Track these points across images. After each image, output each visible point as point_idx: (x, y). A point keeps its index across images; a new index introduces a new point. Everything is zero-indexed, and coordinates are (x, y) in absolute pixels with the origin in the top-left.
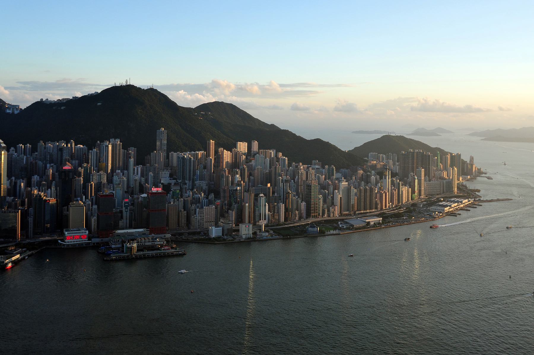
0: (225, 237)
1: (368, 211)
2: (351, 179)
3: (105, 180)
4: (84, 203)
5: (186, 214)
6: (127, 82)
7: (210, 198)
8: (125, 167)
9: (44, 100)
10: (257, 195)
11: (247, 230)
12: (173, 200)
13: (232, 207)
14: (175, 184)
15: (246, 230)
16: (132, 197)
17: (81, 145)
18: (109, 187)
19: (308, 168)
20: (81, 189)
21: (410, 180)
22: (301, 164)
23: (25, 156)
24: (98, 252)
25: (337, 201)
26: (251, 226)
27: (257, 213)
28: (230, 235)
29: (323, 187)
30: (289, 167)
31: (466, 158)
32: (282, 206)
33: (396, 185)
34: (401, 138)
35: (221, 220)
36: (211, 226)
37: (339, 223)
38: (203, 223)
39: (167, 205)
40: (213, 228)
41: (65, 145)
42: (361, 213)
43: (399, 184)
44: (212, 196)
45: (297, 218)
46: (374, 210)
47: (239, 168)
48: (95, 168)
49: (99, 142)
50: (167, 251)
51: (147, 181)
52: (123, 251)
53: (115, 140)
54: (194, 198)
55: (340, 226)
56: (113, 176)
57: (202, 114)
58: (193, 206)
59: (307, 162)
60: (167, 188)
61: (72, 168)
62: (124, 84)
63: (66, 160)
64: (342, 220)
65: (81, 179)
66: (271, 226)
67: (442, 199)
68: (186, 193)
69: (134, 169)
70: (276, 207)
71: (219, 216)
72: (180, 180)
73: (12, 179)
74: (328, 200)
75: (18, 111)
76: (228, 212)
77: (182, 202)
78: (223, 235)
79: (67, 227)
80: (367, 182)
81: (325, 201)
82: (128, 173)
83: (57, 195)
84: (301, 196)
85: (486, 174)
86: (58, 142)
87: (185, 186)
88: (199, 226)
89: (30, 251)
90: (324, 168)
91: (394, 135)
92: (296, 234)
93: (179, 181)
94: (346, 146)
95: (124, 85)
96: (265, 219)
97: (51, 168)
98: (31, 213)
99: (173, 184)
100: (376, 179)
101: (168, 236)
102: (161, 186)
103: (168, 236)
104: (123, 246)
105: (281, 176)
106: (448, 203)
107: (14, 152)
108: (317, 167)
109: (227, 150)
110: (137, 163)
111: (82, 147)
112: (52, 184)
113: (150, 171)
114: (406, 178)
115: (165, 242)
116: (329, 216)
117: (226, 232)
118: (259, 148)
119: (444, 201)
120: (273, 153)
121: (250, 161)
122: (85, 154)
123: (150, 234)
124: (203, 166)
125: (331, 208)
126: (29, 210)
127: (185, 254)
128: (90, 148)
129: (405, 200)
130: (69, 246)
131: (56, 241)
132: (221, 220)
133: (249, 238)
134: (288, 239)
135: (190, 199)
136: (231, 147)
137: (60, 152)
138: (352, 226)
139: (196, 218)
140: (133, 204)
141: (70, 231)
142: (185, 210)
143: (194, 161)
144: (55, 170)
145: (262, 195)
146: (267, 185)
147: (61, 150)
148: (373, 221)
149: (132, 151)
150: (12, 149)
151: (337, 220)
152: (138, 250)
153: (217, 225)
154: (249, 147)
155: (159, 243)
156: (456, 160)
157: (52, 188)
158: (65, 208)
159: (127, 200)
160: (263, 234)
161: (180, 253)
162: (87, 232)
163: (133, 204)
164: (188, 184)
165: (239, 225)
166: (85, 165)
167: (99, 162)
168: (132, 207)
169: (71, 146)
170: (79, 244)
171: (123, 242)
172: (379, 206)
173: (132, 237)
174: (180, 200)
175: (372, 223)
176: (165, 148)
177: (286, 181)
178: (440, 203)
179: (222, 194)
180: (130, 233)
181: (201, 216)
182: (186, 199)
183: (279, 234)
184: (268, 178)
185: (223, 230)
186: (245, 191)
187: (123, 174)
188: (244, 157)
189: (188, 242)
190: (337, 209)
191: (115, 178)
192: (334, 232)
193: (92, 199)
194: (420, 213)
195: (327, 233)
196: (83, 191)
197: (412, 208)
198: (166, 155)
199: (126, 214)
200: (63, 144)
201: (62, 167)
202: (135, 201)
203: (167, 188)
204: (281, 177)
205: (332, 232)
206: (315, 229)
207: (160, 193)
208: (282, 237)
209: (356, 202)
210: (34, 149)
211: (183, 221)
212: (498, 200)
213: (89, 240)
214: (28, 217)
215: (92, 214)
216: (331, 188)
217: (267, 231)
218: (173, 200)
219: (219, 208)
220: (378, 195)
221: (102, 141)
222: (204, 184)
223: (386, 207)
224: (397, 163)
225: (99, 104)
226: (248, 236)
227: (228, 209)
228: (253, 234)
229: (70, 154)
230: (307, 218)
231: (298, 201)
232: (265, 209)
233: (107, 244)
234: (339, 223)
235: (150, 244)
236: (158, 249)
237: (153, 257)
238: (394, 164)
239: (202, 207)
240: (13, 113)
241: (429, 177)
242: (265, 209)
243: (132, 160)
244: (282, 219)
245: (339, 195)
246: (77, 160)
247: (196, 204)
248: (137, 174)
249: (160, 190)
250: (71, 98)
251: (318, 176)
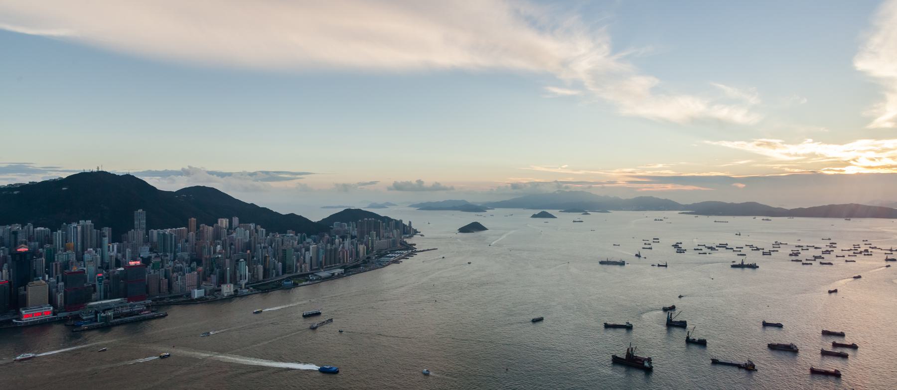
0: (208, 297)
1: (333, 265)
2: (320, 242)
3: (75, 259)
5: (167, 282)
6: (98, 168)
7: (192, 266)
8: (100, 245)
10: (238, 260)
11: (228, 289)
12: (153, 270)
13: (214, 272)
14: (156, 257)
15: (227, 289)
16: (107, 272)
18: (79, 264)
19: (283, 236)
20: (43, 268)
21: (365, 240)
22: (277, 233)
24: (65, 325)
25: (308, 260)
26: (232, 285)
27: (238, 275)
28: (213, 295)
29: (297, 250)
30: (266, 236)
31: (406, 223)
32: (261, 267)
33: (355, 245)
34: (359, 210)
35: (204, 283)
36: (194, 288)
37: (310, 276)
38: (185, 287)
39: (146, 276)
40: (196, 290)
42: (328, 267)
43: (357, 244)
44: (194, 264)
45: (274, 275)
46: (338, 264)
47: (220, 240)
48: (61, 248)
49: (64, 224)
50: (147, 315)
51: (124, 256)
52: (96, 321)
53: (85, 221)
54: (176, 268)
55: (311, 278)
56: (83, 254)
57: (183, 197)
58: (175, 274)
59: (283, 231)
60: (146, 261)
61: (30, 249)
62: (95, 170)
63: (22, 243)
64: (312, 273)
65: (43, 260)
66: (251, 284)
67: (389, 252)
68: (167, 263)
69: (109, 247)
70: (256, 269)
71: (201, 281)
72: (161, 253)
74: (300, 259)
76: (210, 277)
77: (164, 272)
78: (205, 295)
79: (25, 305)
80: (332, 242)
81: (298, 260)
82: (102, 250)
83: (10, 276)
84: (277, 258)
85: (420, 232)
86: (10, 225)
87: (167, 258)
88: (181, 290)
90: (297, 235)
91: (353, 208)
92: (273, 288)
93: (160, 254)
94: (315, 217)
95: (95, 172)
96: (245, 279)
99: (153, 257)
100: (339, 241)
101: (149, 301)
102: (141, 259)
103: (149, 301)
104: (97, 316)
105: (260, 244)
106: (393, 255)
108: (291, 235)
109: (210, 226)
110: (113, 240)
111: (44, 231)
112: (3, 266)
113: (128, 247)
114: (362, 239)
115: (145, 308)
116: (301, 271)
117: (208, 292)
118: (240, 222)
119: (390, 253)
120: (252, 226)
121: (232, 234)
123: (128, 302)
124: (184, 240)
125: (303, 265)
127: (167, 315)
128: (54, 229)
129: (361, 254)
131: (10, 321)
132: (204, 283)
133: (230, 296)
134: (266, 292)
135: (170, 268)
136: (212, 222)
137: (13, 236)
138: (321, 277)
139: (178, 284)
140: (107, 278)
142: (166, 278)
143: (175, 236)
144: (7, 252)
145: (243, 260)
146: (246, 252)
147: (15, 233)
148: (337, 271)
149: (107, 231)
151: (309, 274)
152: (114, 318)
153: (199, 288)
154: (231, 223)
155: (138, 309)
156: (398, 224)
157: (4, 271)
158: (21, 288)
159: (101, 275)
160: (244, 291)
161: (161, 315)
162: (52, 308)
163: (107, 278)
164: (169, 256)
165: (221, 286)
166: (48, 246)
167: (66, 242)
168: (107, 280)
169: (29, 228)
170: (41, 320)
171: (96, 313)
172: (342, 261)
173: (106, 308)
174: (161, 270)
175: (336, 274)
176: (144, 226)
177: (264, 248)
178: (388, 255)
179: (204, 261)
180: (105, 303)
181: (183, 282)
182: (167, 269)
183: (258, 289)
184: (248, 246)
185: (205, 292)
186: (227, 258)
187: (96, 252)
188: (226, 230)
189: (169, 304)
190: (308, 266)
191: (87, 256)
192: (306, 283)
193: (58, 277)
194: (373, 263)
195: (299, 284)
196: (45, 270)
197: (367, 260)
198: (145, 232)
199: (100, 287)
201: (16, 250)
202: (111, 275)
203: (146, 261)
204: (259, 245)
205: (304, 283)
206: (290, 282)
207: (139, 266)
208: (260, 291)
209: (324, 259)
211: (165, 287)
212: (428, 250)
213: (54, 315)
215: (57, 291)
216: (303, 250)
217: (248, 288)
218: (153, 270)
219: (201, 274)
220: (341, 253)
221: (69, 222)
222: (186, 255)
223: (347, 261)
224: (356, 229)
225: (64, 189)
226: (229, 293)
227: (211, 274)
228: (234, 291)
229: (27, 236)
230: (283, 274)
231: (275, 262)
232: (244, 269)
233: (77, 318)
234: (310, 276)
235: (129, 310)
236: (138, 314)
237: (132, 322)
238: (353, 230)
239: (184, 274)
241: (379, 238)
242: (244, 269)
243: (106, 240)
244: (261, 277)
245: (309, 255)
246: (37, 241)
247: (178, 272)
248: (113, 250)
249: (138, 263)
251: (293, 242)
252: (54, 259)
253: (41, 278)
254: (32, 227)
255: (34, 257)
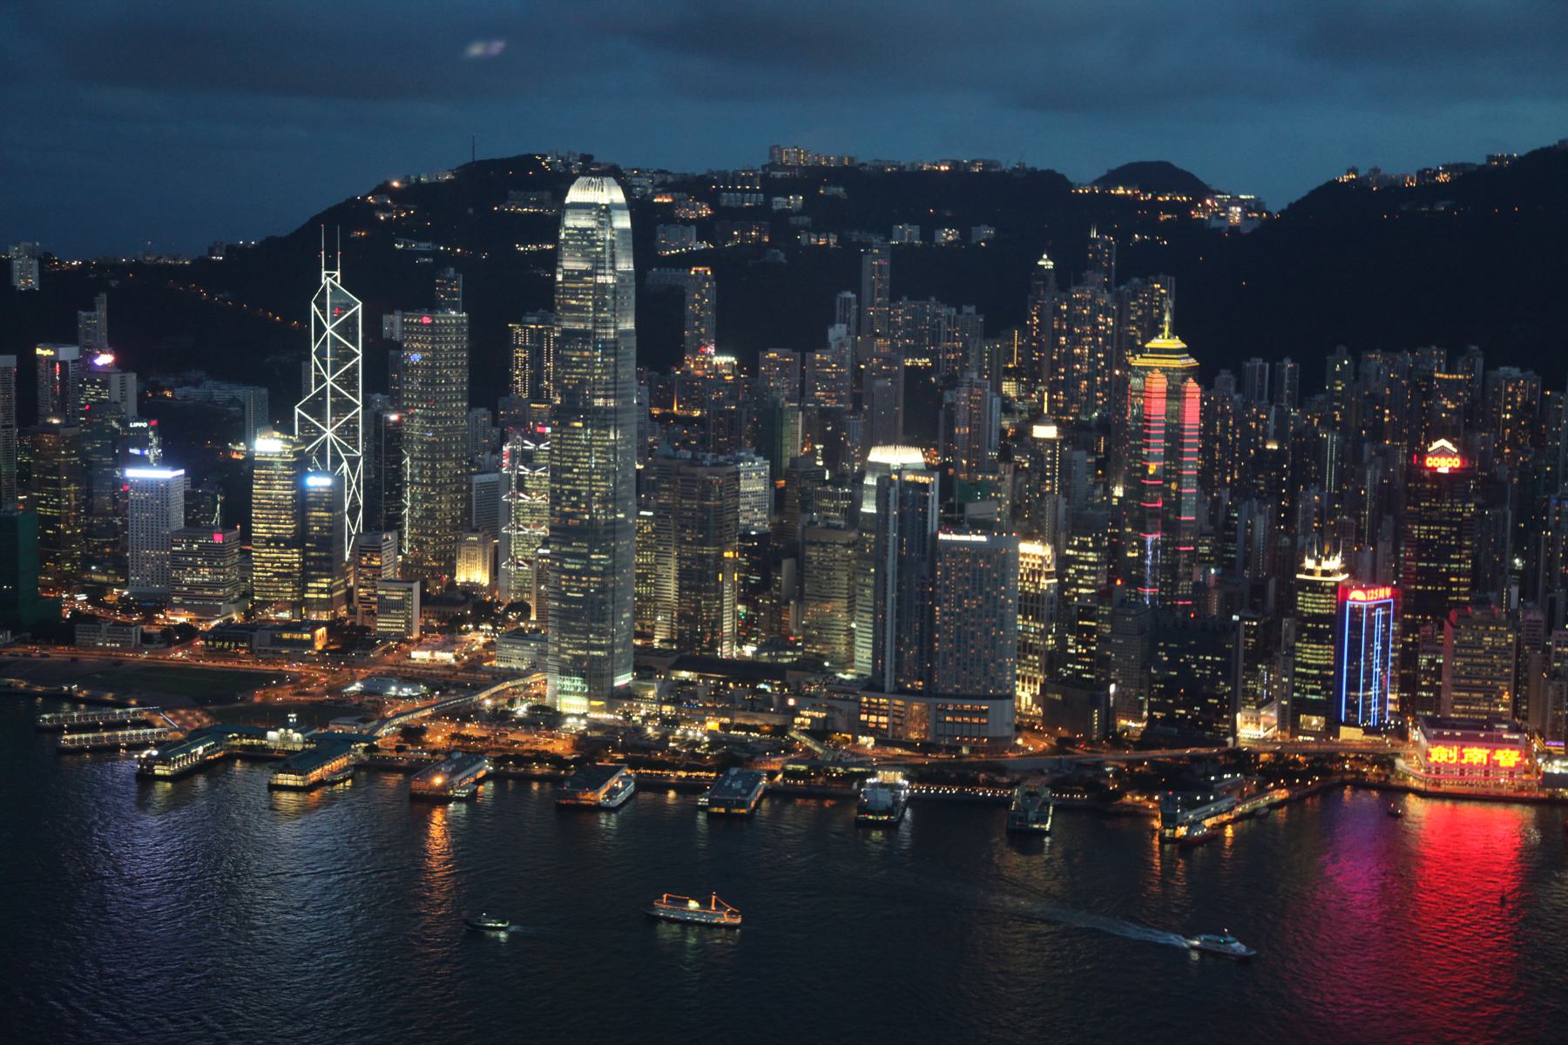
4: (1512, 615)
9: (1362, 173)
17: (1514, 366)
23: (1273, 408)
41: (1443, 366)
73: (1219, 498)
75: (1257, 224)
86: (1412, 352)
89: (1278, 786)
97: (1380, 460)
98: (1287, 636)
107: (1232, 389)
112: (1379, 526)
122: (1526, 405)
126: (1281, 625)
130: (1439, 785)
141: (1446, 727)
147: (1425, 389)
150: (1225, 375)
157: (1381, 545)
158: (1428, 628)
193: (1553, 602)
200: (1436, 361)
201: (1424, 459)
210: (1311, 384)
214: (1276, 654)
240: (1234, 229)
250: (1482, 161)
252: (1546, 512)
253: (1492, 595)
254: (1480, 362)
255: (1480, 500)
